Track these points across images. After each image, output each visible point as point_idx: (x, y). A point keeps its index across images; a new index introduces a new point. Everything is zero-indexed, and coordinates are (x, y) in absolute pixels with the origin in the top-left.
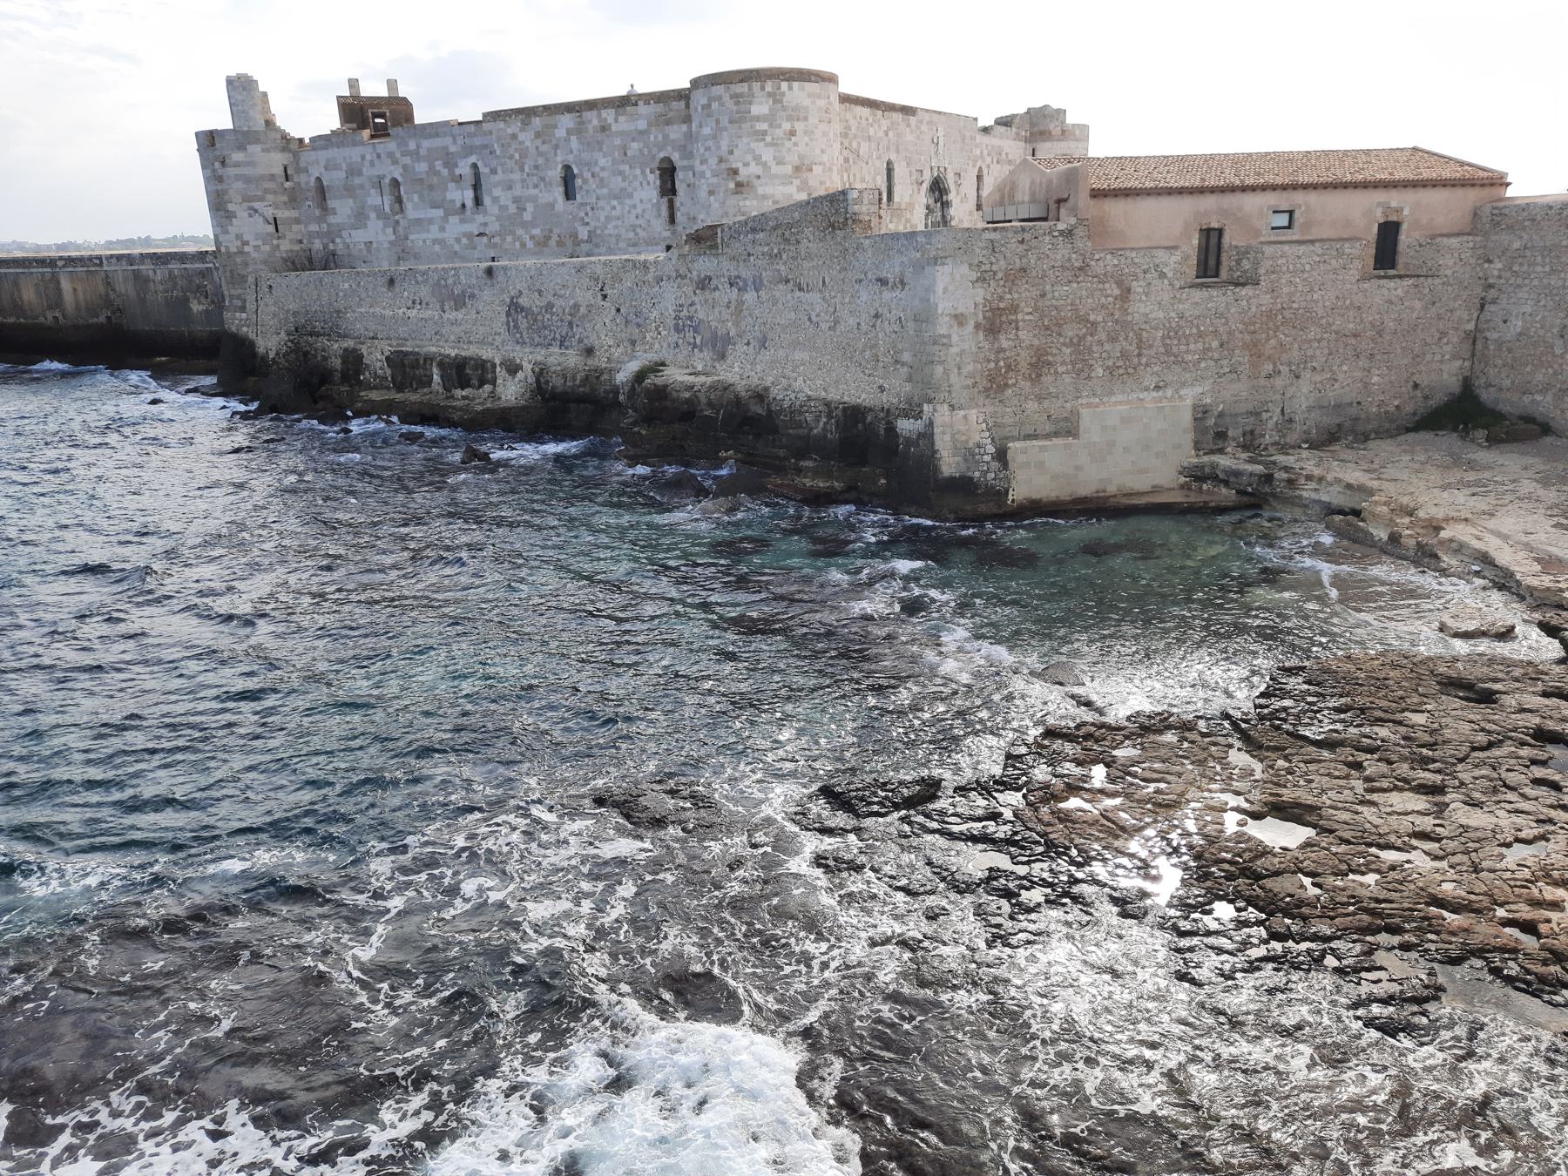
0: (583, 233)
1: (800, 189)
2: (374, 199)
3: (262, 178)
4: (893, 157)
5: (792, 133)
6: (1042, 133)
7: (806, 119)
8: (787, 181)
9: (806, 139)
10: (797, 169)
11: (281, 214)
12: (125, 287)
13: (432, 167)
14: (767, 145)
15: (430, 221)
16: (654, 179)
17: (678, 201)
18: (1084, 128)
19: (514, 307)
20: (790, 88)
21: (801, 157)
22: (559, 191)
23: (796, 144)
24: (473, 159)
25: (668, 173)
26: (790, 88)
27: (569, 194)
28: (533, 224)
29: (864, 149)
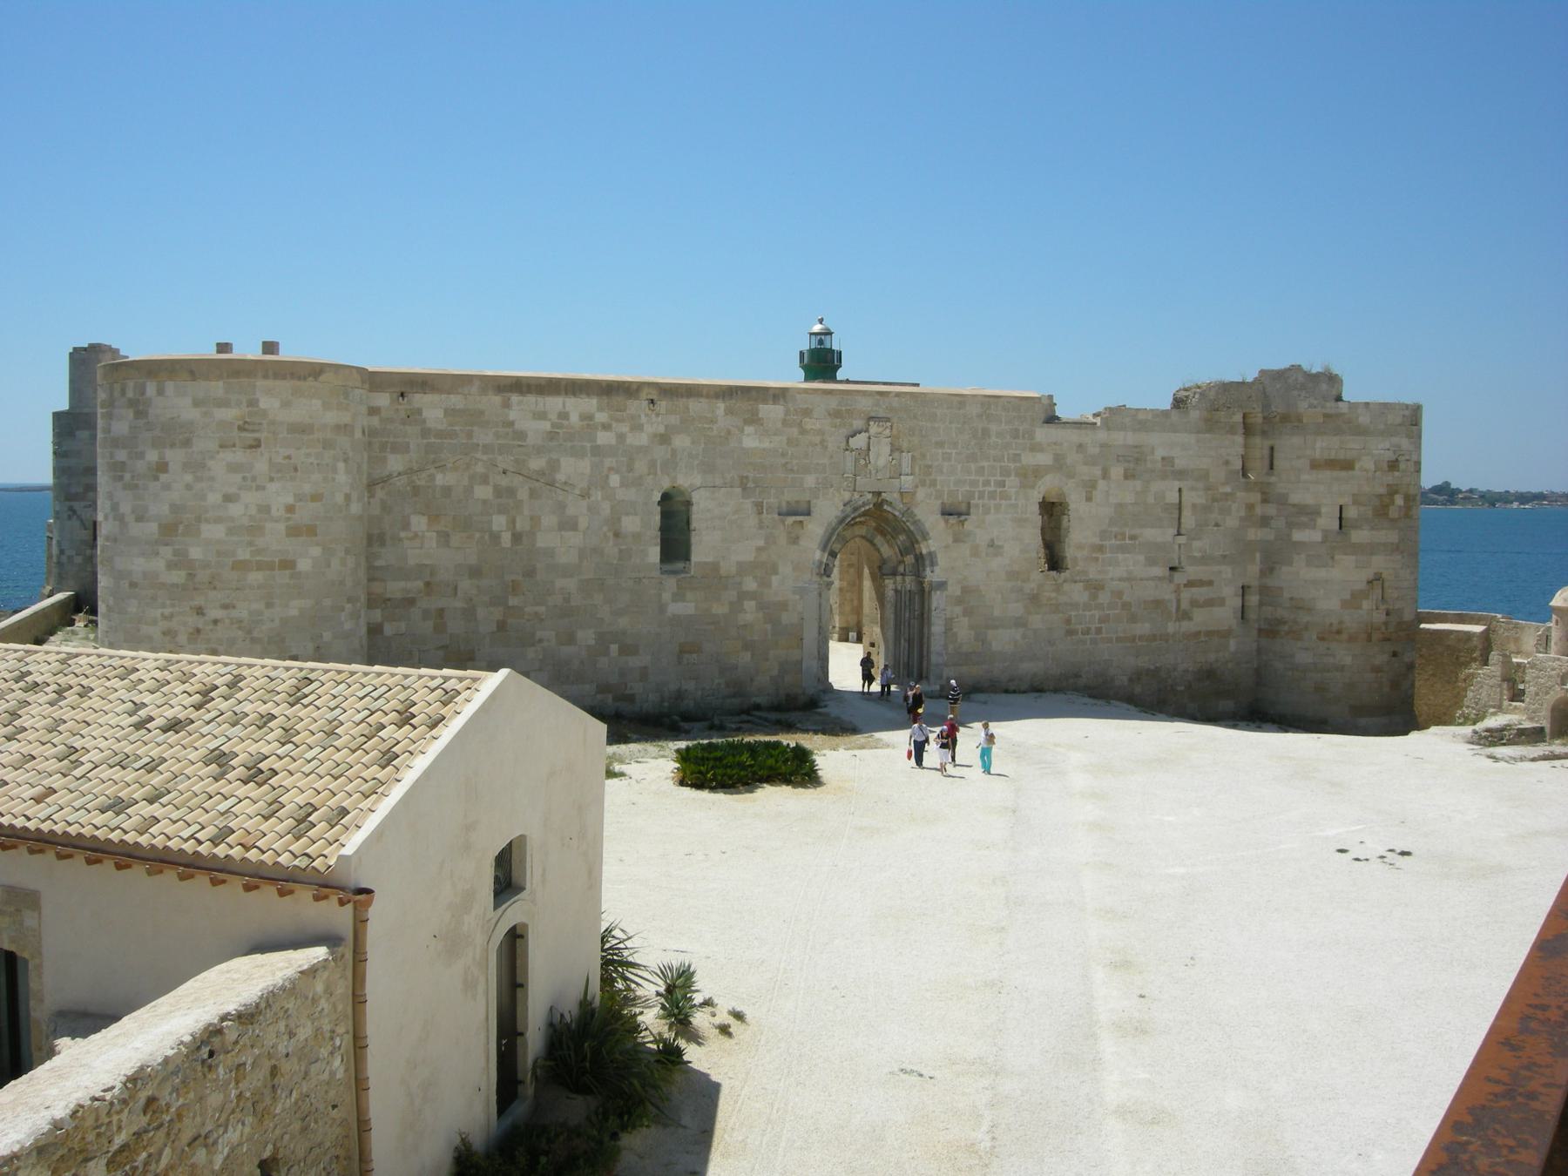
1: (171, 566)
4: (686, 480)
5: (162, 467)
6: (1285, 419)
7: (187, 443)
9: (189, 478)
10: (169, 530)
14: (125, 487)
20: (161, 392)
21: (175, 508)
23: (167, 487)
26: (161, 392)
29: (573, 468)
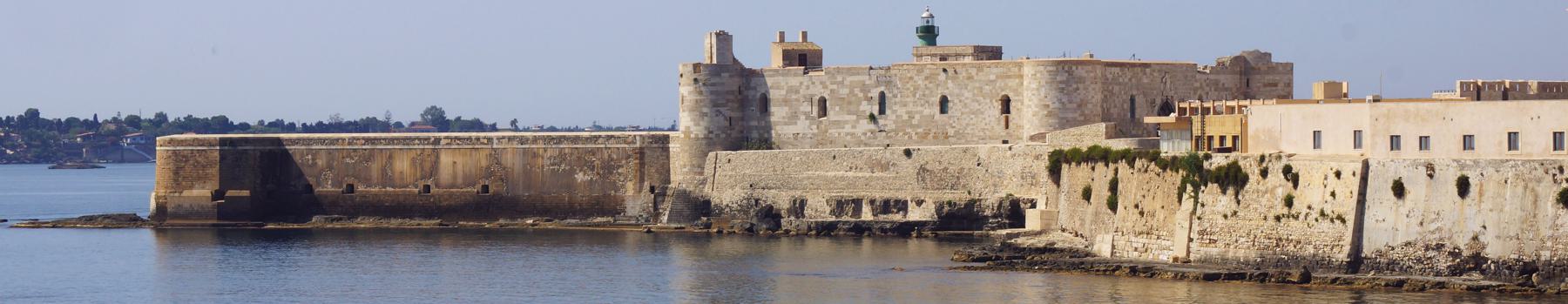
0: (951, 132)
2: (806, 107)
3: (727, 93)
8: (1075, 110)
10: (1080, 106)
11: (733, 115)
12: (512, 160)
13: (852, 92)
15: (846, 122)
16: (998, 106)
17: (1011, 116)
18: (1288, 68)
19: (923, 169)
22: (938, 109)
24: (882, 89)
25: (1006, 104)
27: (943, 110)
28: (918, 126)
